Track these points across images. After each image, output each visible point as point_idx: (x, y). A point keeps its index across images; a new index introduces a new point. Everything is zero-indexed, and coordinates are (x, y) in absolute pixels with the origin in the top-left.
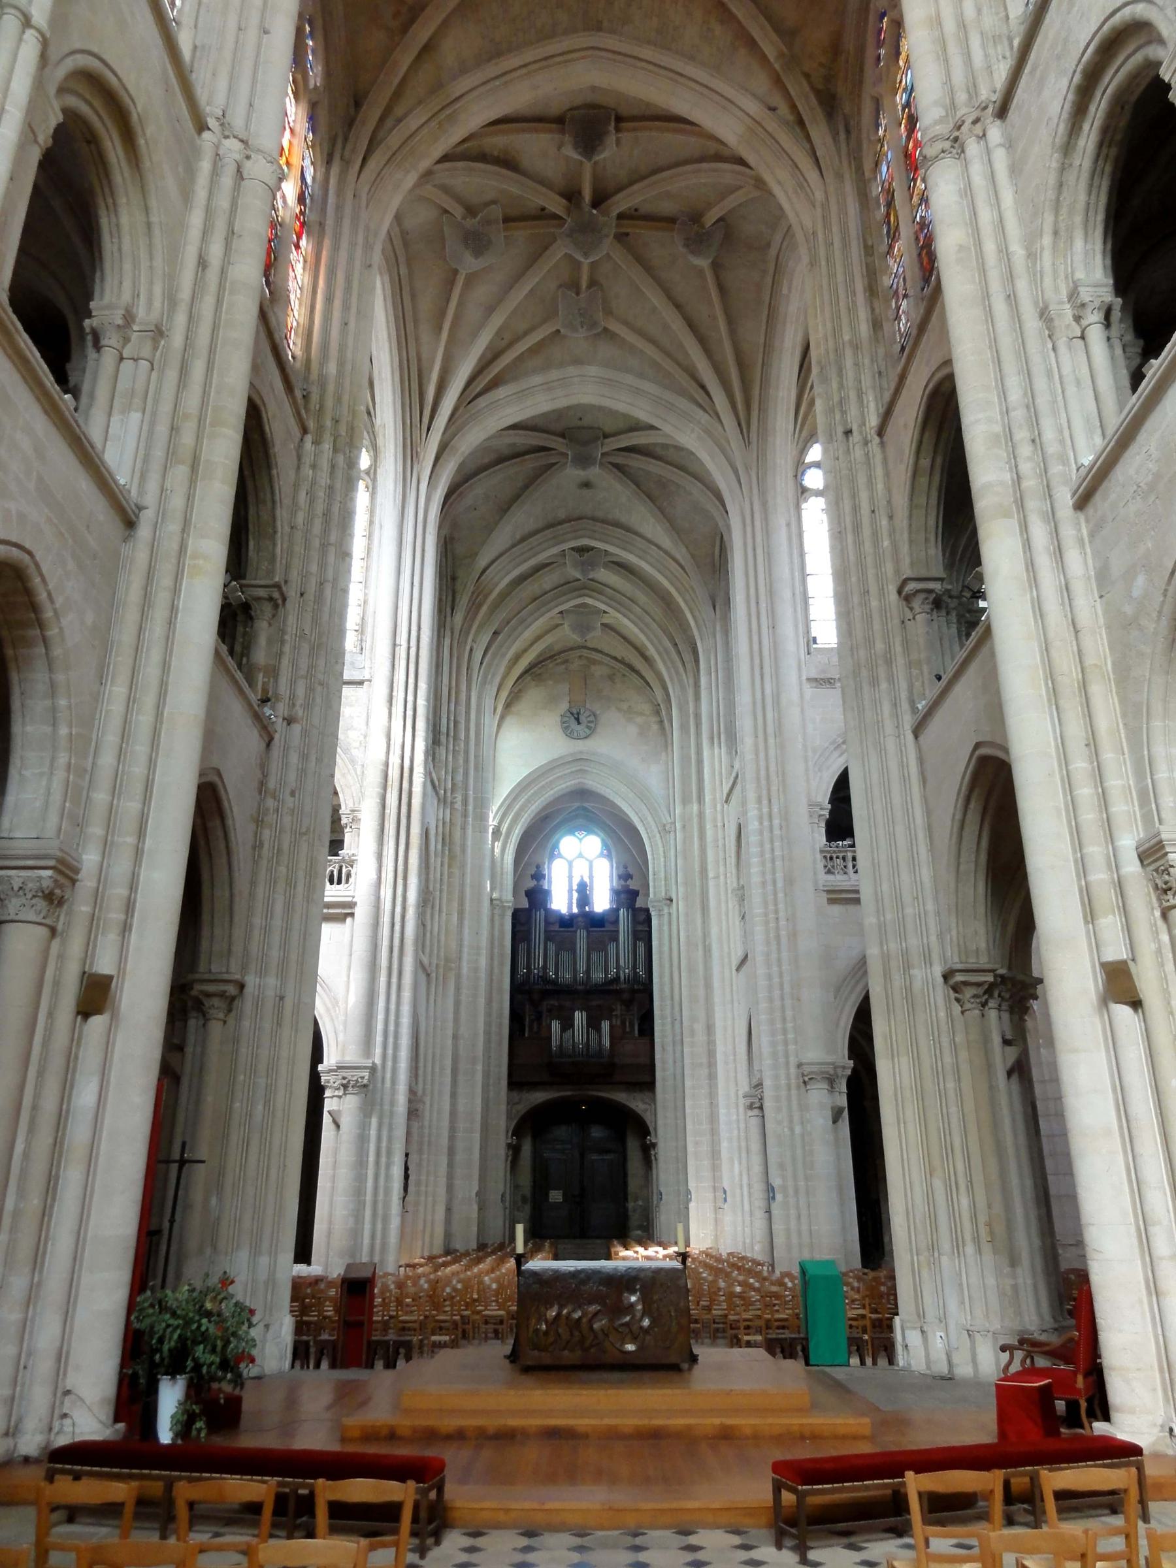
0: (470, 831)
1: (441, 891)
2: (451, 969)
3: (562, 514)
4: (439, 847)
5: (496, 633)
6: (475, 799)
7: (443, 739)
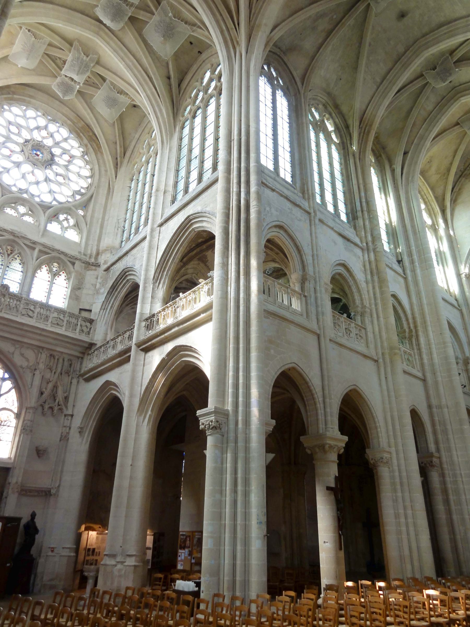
0: (418, 271)
1: (376, 305)
2: (395, 354)
3: (401, 49)
4: (369, 277)
5: (405, 153)
6: (419, 252)
7: (359, 214)
